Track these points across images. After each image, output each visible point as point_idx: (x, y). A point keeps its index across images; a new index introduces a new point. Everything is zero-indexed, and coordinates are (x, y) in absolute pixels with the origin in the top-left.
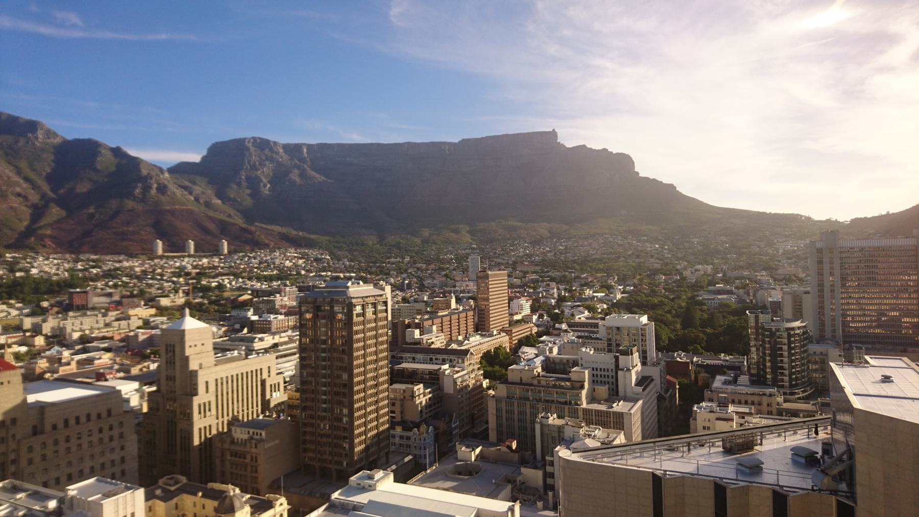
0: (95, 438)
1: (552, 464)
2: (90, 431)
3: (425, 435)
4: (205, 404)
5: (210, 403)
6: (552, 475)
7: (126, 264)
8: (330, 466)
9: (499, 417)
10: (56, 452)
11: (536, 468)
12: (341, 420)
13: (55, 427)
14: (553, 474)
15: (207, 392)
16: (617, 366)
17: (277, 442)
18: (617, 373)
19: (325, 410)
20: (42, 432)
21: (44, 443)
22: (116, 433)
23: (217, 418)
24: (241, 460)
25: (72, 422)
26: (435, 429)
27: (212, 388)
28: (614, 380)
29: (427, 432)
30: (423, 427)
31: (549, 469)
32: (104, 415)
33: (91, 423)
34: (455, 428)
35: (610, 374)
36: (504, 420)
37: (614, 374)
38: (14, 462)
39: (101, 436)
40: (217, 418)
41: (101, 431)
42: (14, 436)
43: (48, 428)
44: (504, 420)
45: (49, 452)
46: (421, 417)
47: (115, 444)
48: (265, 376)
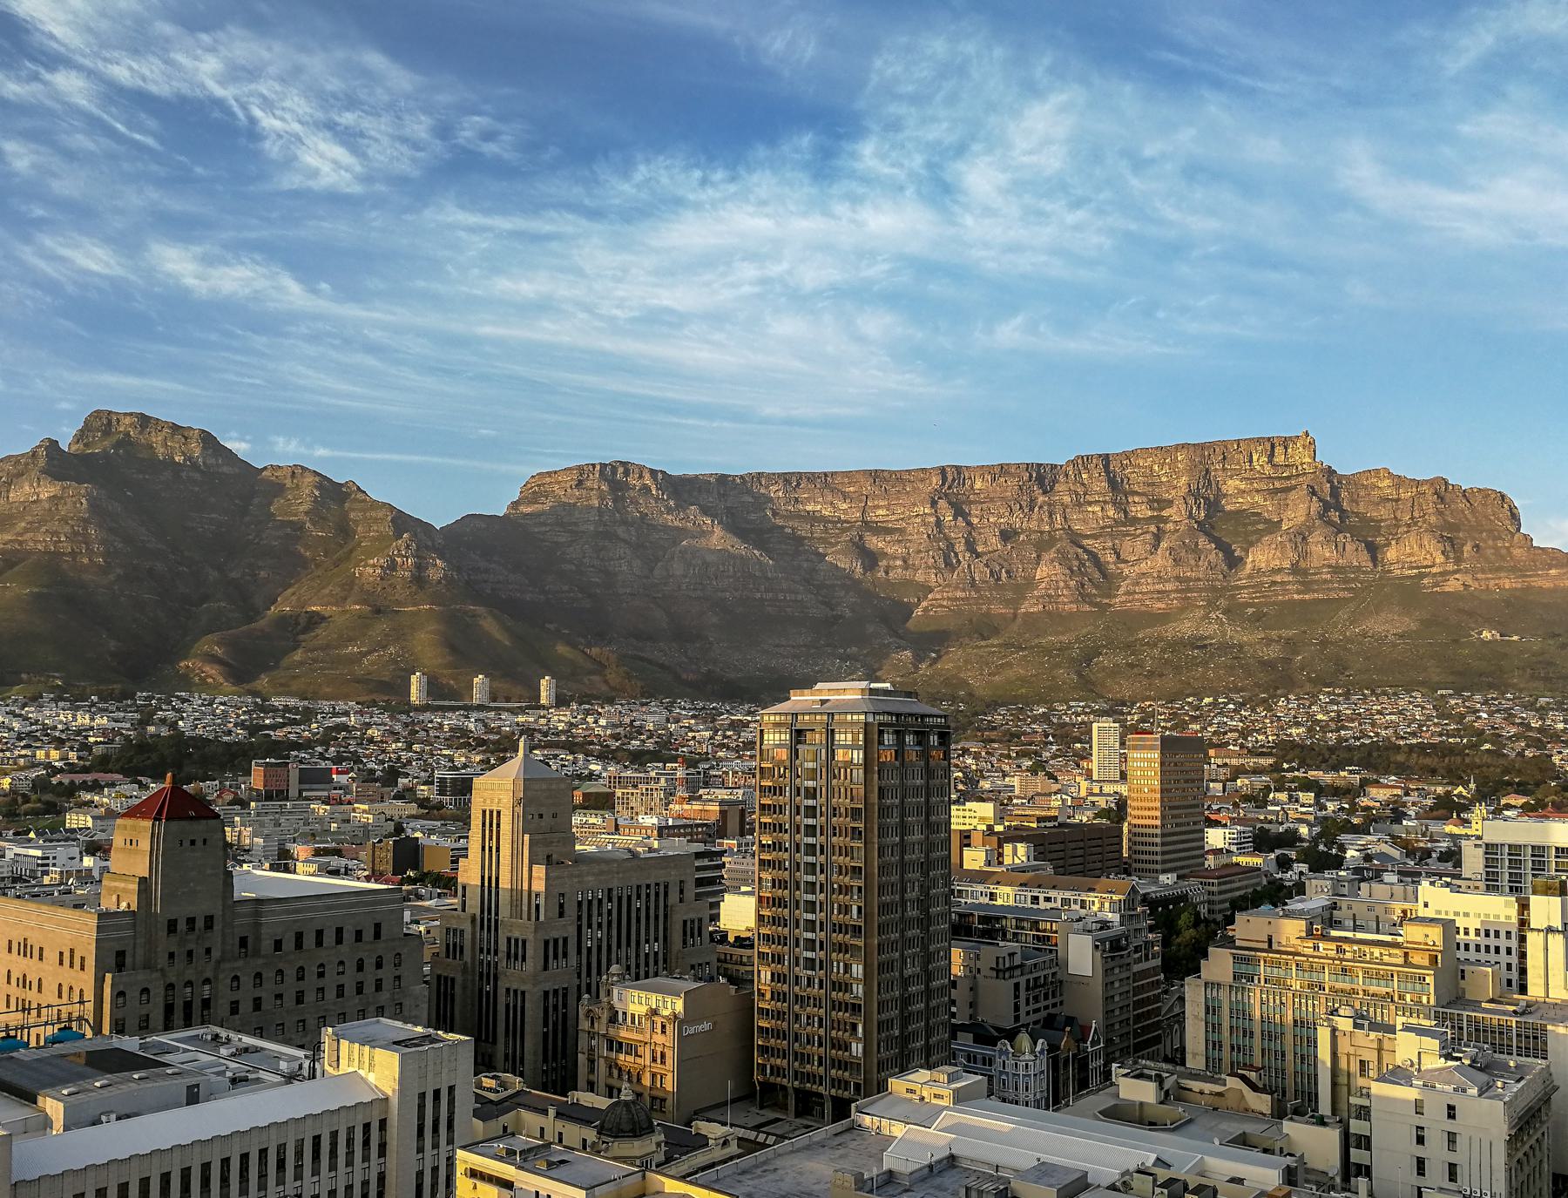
0: (349, 981)
1: (1364, 1113)
2: (342, 963)
3: (1028, 1056)
4: (556, 941)
5: (565, 940)
6: (1365, 1142)
7: (353, 720)
8: (821, 1089)
9: (1213, 1027)
10: (279, 996)
11: (1322, 1122)
12: (847, 988)
13: (278, 945)
14: (1368, 1139)
15: (561, 915)
16: (1523, 923)
17: (706, 1026)
18: (1523, 939)
19: (810, 964)
20: (257, 953)
21: (259, 975)
22: (387, 973)
23: (579, 976)
24: (630, 1059)
25: (309, 941)
26: (1053, 1048)
27: (571, 911)
28: (1514, 959)
29: (1032, 1052)
30: (1024, 1040)
31: (1356, 1126)
32: (368, 935)
33: (344, 948)
34: (1096, 1054)
35: (1503, 943)
36: (1226, 1033)
37: (1514, 943)
38: (206, 1004)
39: (360, 977)
40: (579, 976)
41: (360, 967)
42: (208, 951)
43: (267, 945)
44: (1226, 1033)
45: (266, 993)
46: (1017, 1019)
47: (384, 997)
48: (674, 897)
